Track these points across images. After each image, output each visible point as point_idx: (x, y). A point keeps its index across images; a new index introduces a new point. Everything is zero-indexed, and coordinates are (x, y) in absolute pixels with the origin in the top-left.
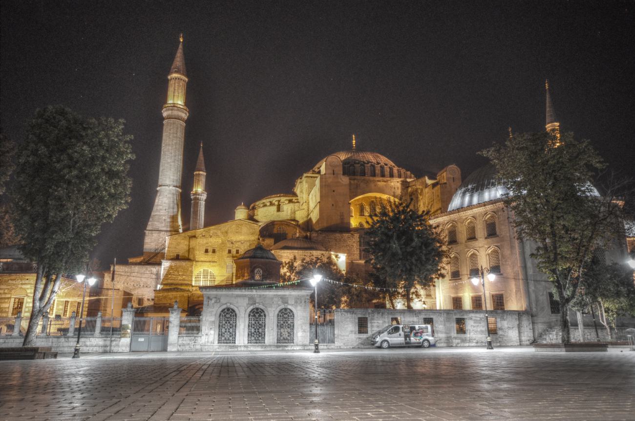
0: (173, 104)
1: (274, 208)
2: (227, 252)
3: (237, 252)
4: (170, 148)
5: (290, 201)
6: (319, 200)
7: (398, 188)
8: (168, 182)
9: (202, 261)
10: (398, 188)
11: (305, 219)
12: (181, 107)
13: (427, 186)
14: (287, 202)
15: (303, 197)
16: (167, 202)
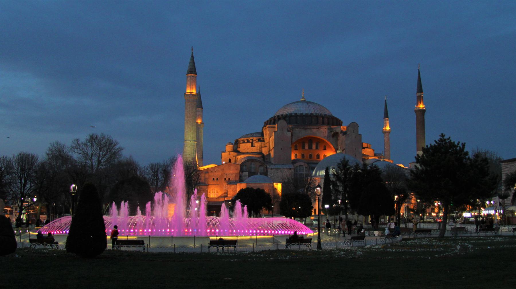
0: (190, 93)
1: (250, 144)
2: (224, 179)
3: (229, 179)
4: (190, 119)
5: (259, 140)
6: (274, 146)
7: (325, 132)
8: (190, 139)
9: (212, 185)
11: (268, 153)
12: (195, 94)
13: (342, 132)
14: (257, 141)
15: (267, 138)
16: (190, 150)
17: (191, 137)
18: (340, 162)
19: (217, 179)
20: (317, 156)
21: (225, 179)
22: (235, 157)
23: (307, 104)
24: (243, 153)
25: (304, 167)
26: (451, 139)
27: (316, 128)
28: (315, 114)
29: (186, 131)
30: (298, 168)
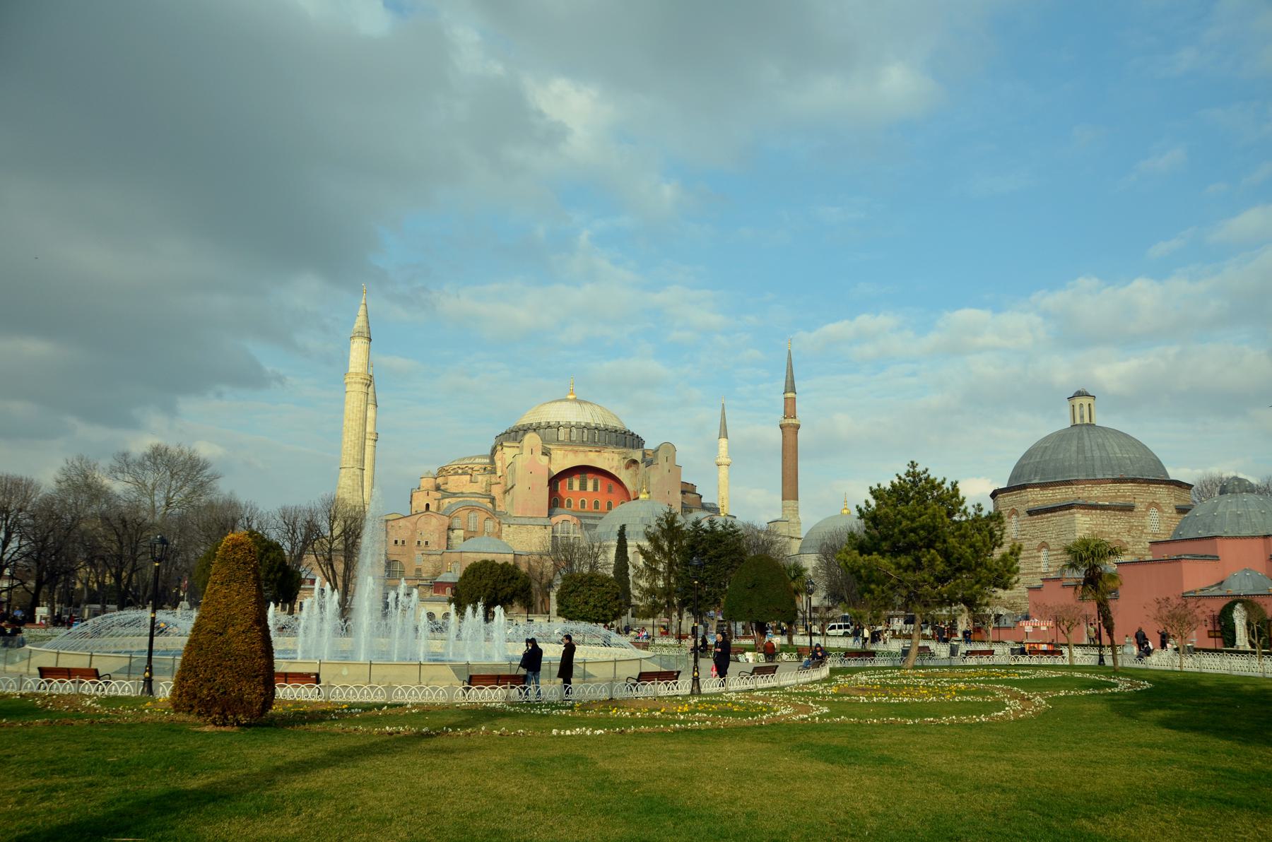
7: (613, 459)
10: (613, 459)
14: (482, 471)
17: (354, 458)
18: (662, 516)
19: (403, 542)
20: (595, 504)
21: (419, 542)
22: (437, 501)
23: (578, 405)
24: (454, 495)
25: (572, 523)
26: (928, 472)
27: (596, 451)
28: (593, 425)
29: (345, 446)
30: (560, 525)
